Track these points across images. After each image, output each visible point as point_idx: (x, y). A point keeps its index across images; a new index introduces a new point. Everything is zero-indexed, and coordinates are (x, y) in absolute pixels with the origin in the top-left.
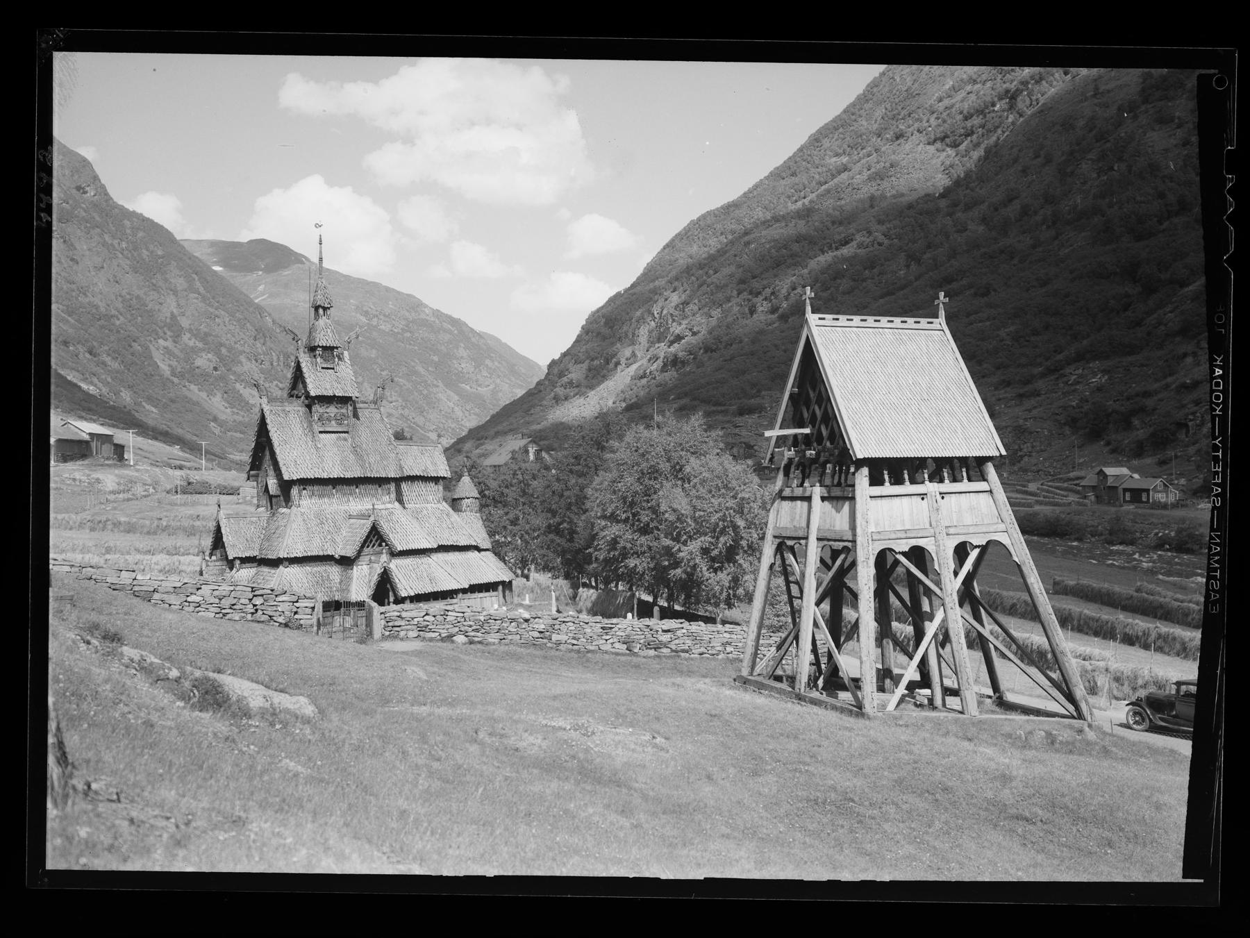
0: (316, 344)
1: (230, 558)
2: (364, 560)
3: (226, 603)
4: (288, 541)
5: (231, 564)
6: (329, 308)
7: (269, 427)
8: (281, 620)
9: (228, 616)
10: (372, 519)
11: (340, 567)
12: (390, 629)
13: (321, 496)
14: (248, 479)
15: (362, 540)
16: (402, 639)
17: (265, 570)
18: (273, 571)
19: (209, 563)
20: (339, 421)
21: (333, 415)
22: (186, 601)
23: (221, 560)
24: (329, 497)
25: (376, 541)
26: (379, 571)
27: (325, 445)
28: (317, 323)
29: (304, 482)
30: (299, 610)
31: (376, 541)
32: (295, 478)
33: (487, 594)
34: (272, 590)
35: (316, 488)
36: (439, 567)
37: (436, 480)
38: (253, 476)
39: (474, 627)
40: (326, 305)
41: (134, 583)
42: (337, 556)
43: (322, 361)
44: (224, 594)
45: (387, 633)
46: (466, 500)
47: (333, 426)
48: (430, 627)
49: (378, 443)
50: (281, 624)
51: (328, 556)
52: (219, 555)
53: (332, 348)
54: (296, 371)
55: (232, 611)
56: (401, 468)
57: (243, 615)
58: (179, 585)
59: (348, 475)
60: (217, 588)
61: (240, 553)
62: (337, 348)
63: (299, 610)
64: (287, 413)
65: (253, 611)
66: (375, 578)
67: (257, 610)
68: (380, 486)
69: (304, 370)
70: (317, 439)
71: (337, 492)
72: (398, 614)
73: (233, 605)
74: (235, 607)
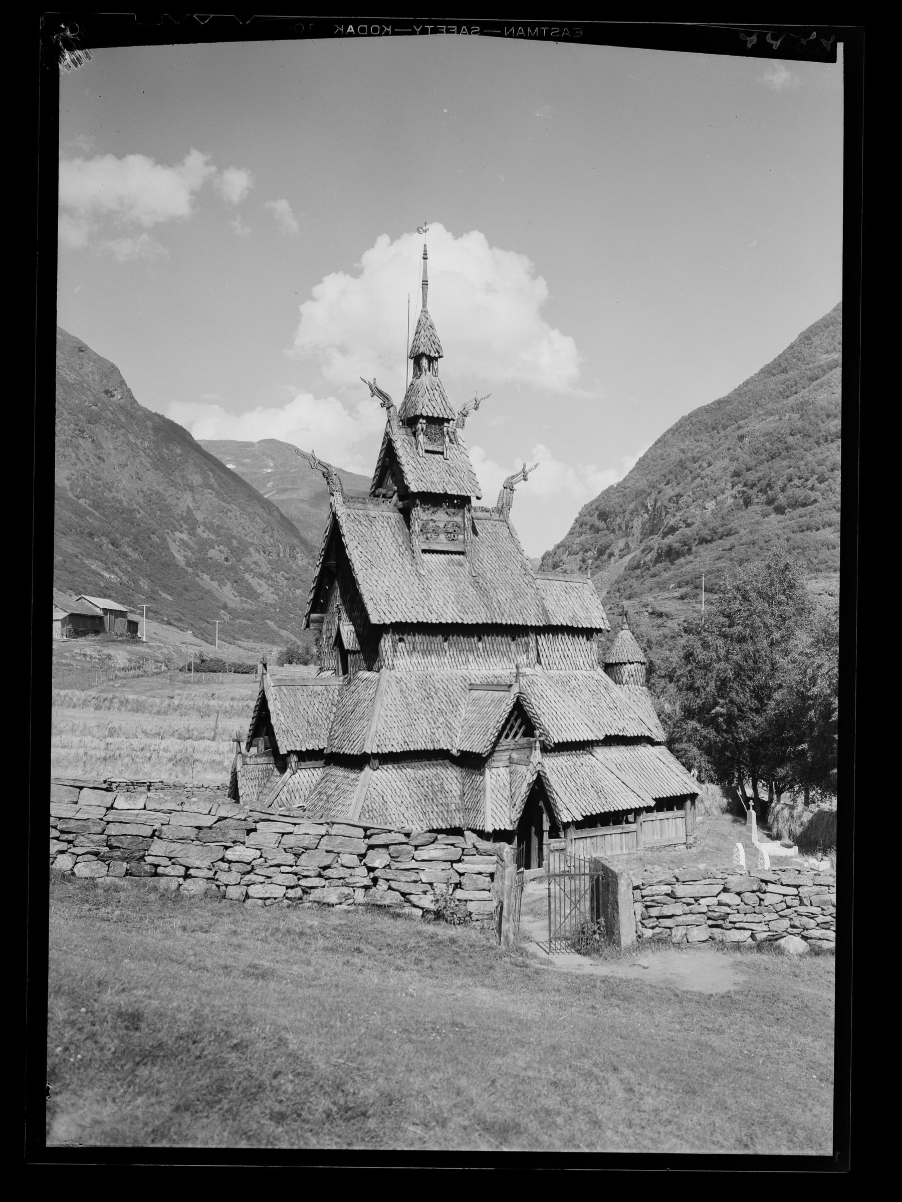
0: (418, 413)
1: (283, 751)
2: (500, 759)
3: (310, 863)
4: (377, 725)
5: (281, 762)
6: (436, 359)
7: (346, 540)
8: (427, 902)
9: (315, 895)
10: (515, 690)
11: (458, 769)
12: (650, 923)
13: (426, 652)
14: (308, 626)
15: (500, 726)
16: (678, 945)
17: (339, 772)
18: (353, 776)
19: (248, 760)
20: (451, 535)
21: (442, 525)
22: (222, 860)
23: (266, 754)
24: (438, 655)
25: (520, 727)
26: (531, 778)
27: (431, 572)
28: (418, 381)
29: (402, 629)
30: (464, 880)
31: (520, 727)
32: (388, 622)
33: (670, 814)
34: (407, 835)
35: (418, 638)
36: (606, 771)
37: (588, 633)
38: (315, 621)
39: (820, 919)
40: (433, 354)
41: (110, 818)
42: (454, 752)
43: (426, 440)
44: (306, 843)
45: (648, 933)
46: (628, 666)
47: (442, 542)
48: (731, 918)
49: (509, 572)
50: (426, 911)
51: (441, 750)
52: (262, 747)
53: (437, 422)
54: (386, 456)
55: (323, 882)
56: (545, 612)
57: (347, 891)
58: (207, 821)
59: (469, 619)
60: (290, 828)
61: (297, 744)
62: (448, 421)
63: (464, 880)
64: (371, 520)
65: (367, 882)
66: (523, 791)
67: (375, 880)
68: (513, 640)
69: (400, 452)
70: (419, 561)
71: (450, 645)
72: (667, 889)
73: (325, 868)
74: (327, 873)
